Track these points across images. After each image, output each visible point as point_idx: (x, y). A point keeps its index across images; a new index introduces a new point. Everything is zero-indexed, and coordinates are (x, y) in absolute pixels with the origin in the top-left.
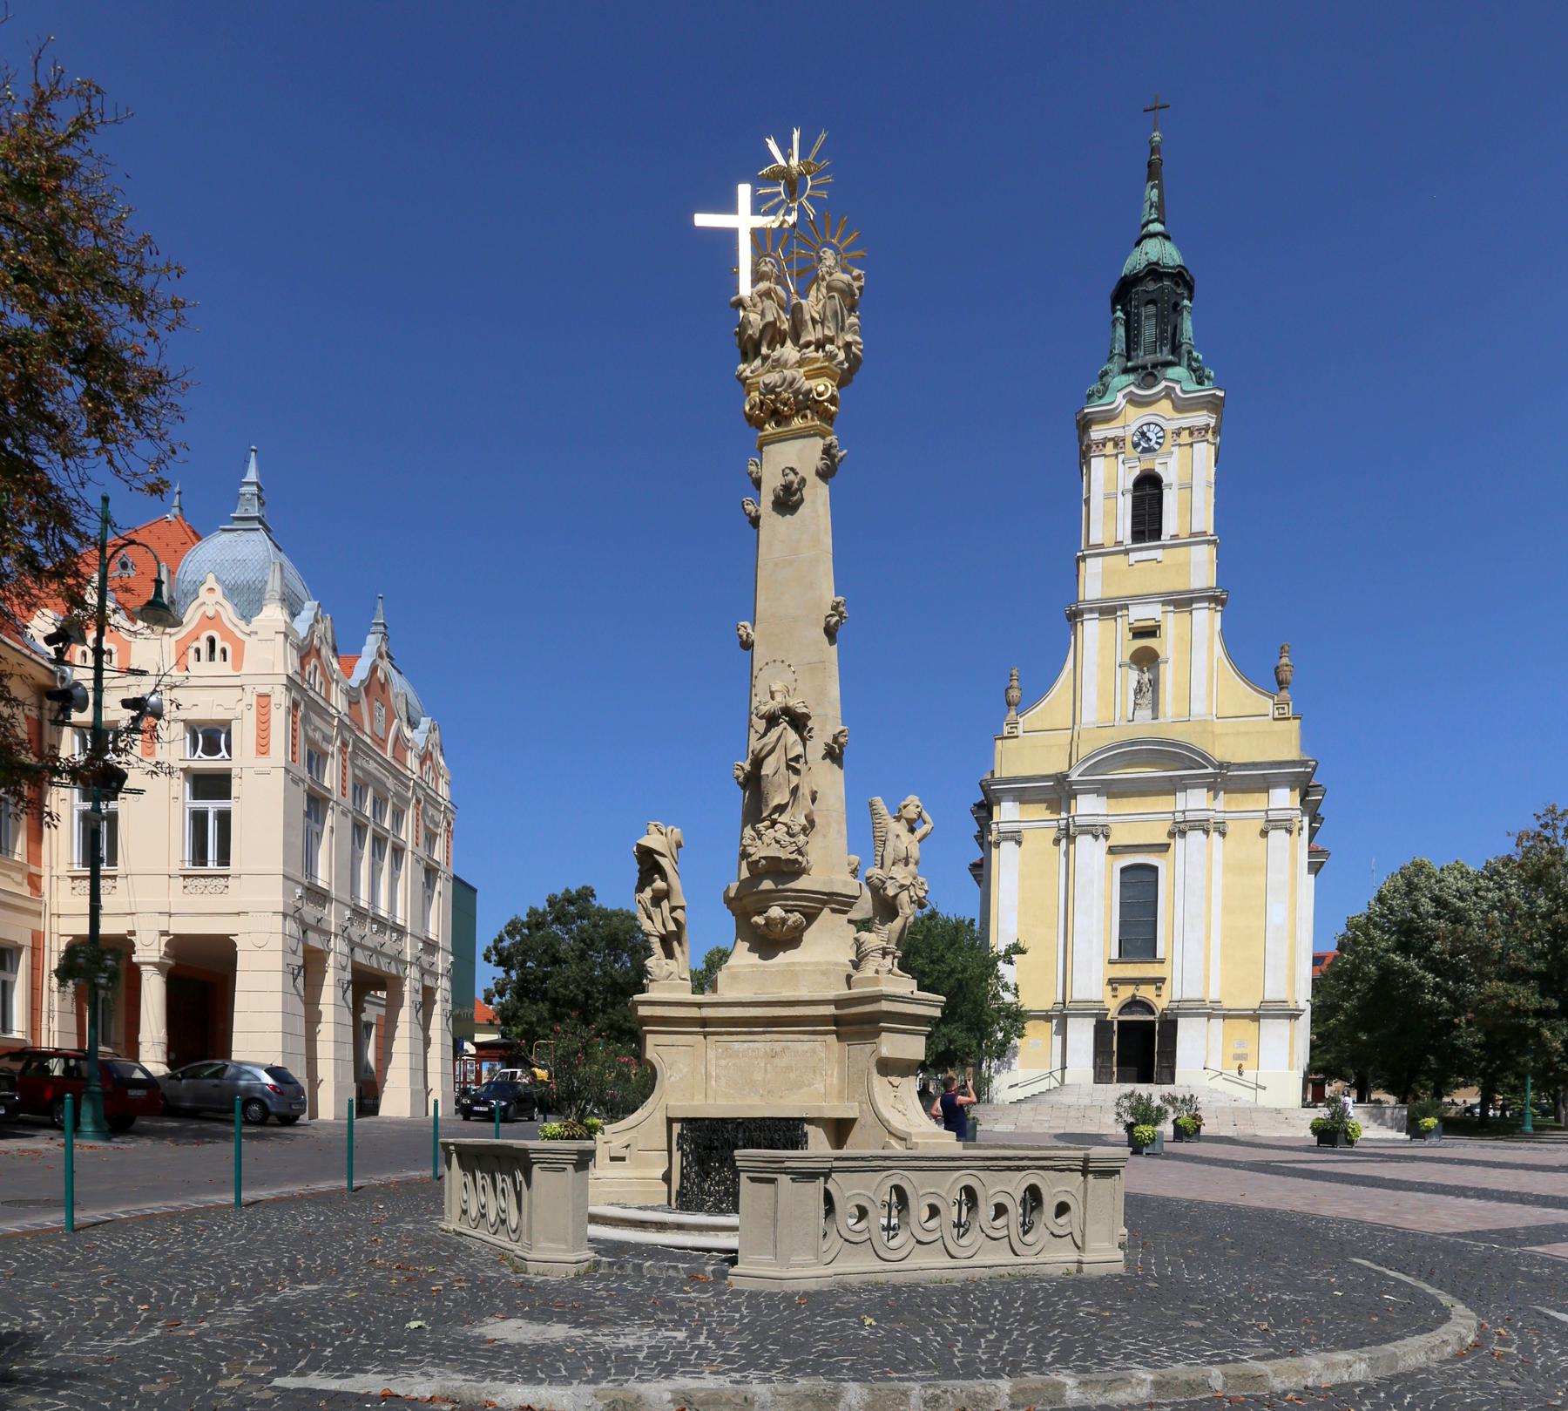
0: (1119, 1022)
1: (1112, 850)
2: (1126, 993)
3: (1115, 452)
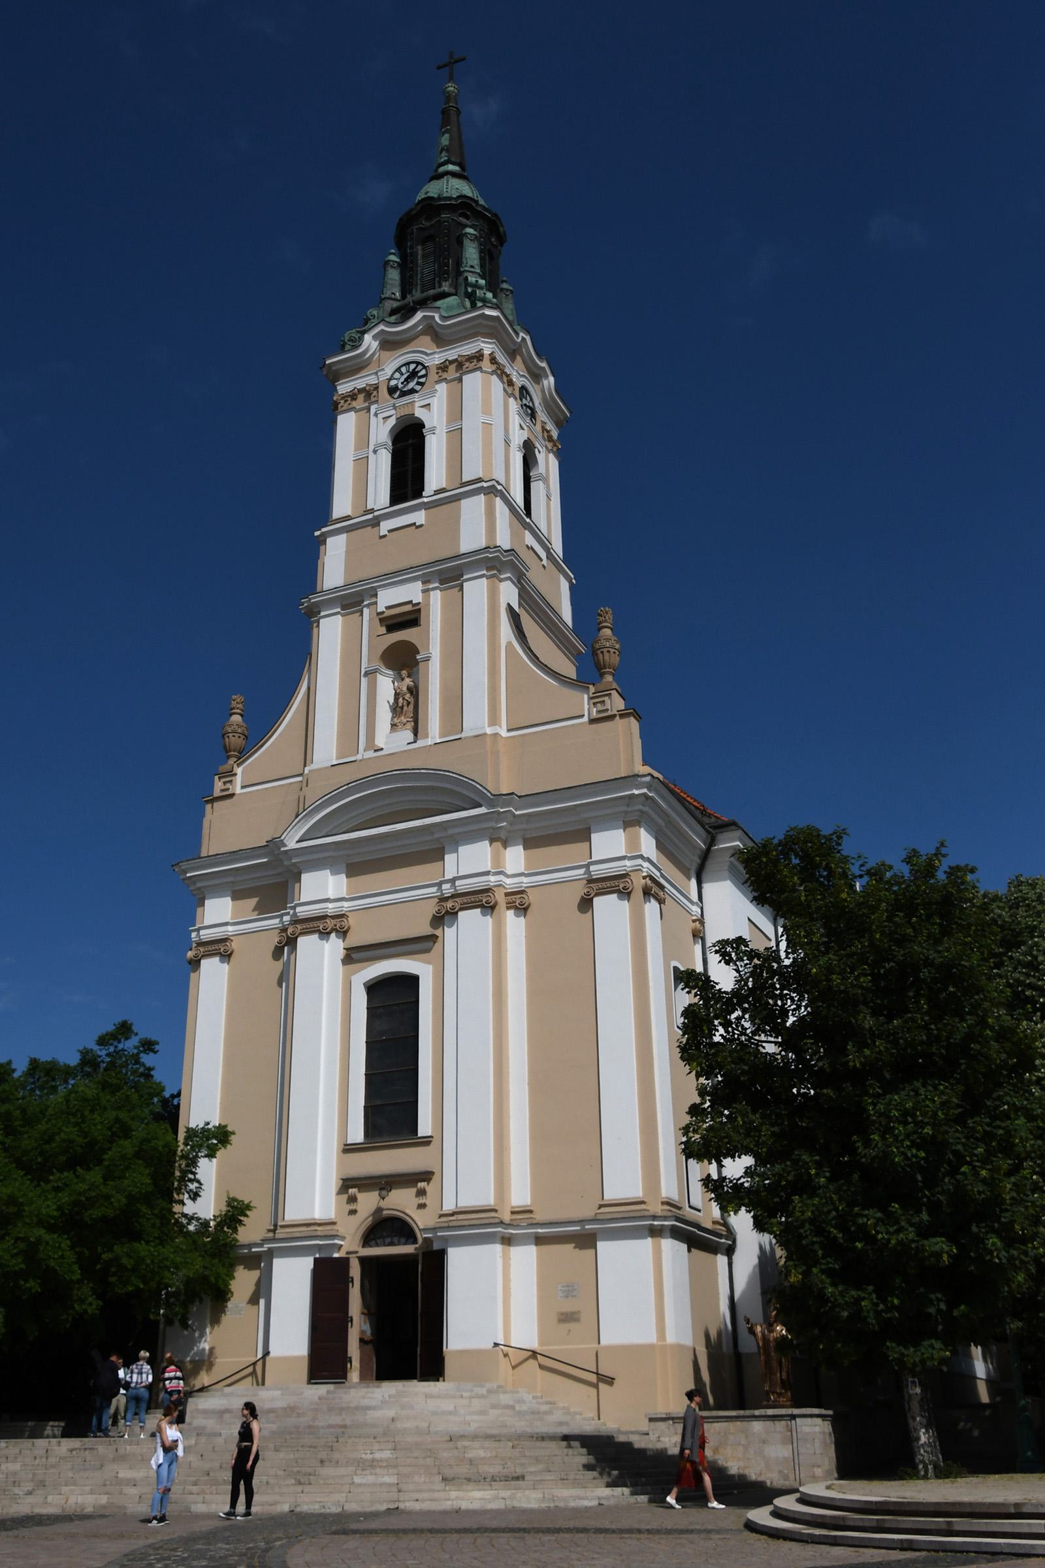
0: (363, 1261)
1: (354, 956)
2: (368, 1202)
3: (367, 404)
